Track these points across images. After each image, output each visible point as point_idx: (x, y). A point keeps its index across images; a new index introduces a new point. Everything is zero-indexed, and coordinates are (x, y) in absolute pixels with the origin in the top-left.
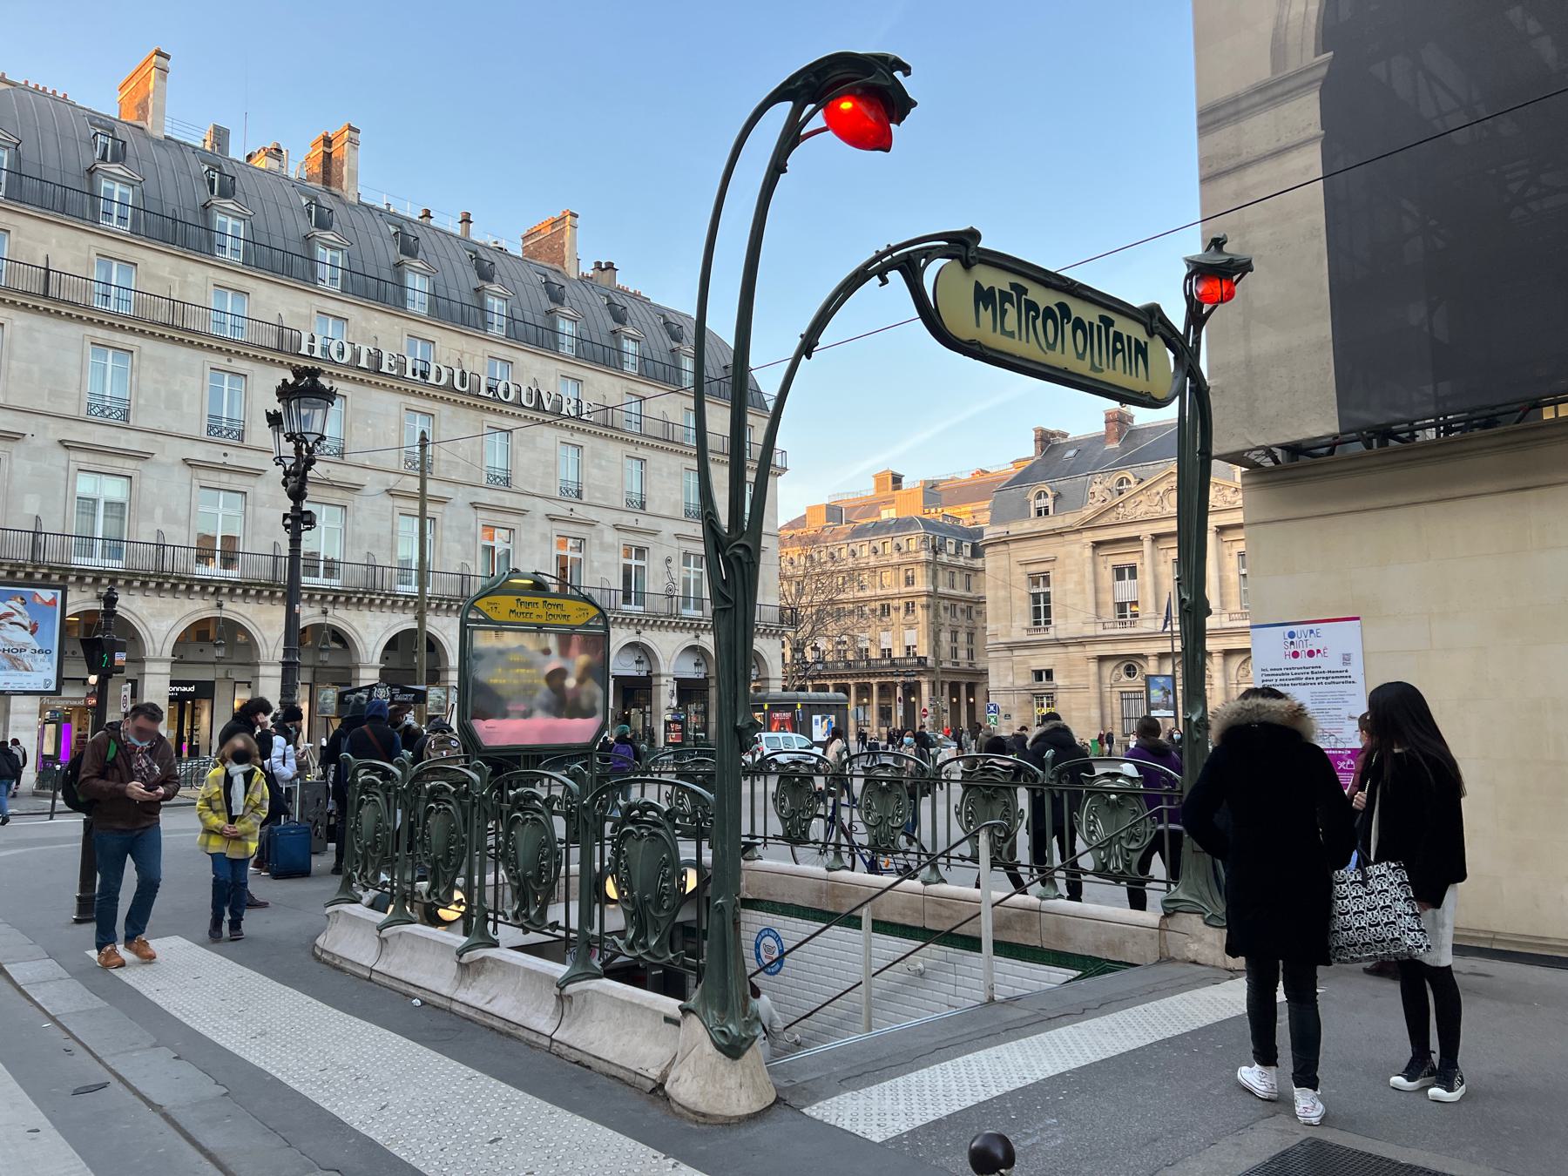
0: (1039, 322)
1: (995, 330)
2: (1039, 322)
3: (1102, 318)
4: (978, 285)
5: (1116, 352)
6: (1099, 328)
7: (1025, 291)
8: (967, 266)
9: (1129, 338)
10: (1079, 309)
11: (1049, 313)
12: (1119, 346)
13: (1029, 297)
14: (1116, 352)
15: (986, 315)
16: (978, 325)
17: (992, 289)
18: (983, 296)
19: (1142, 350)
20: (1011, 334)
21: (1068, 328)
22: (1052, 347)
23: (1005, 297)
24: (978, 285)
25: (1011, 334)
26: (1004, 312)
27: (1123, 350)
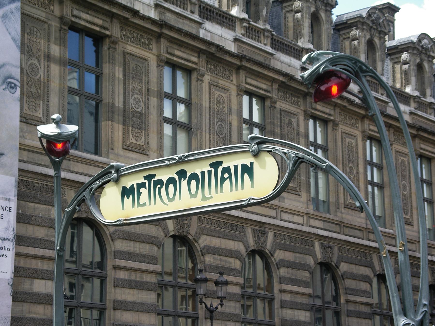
0: (163, 190)
2: (163, 190)
3: (211, 165)
4: (124, 188)
5: (223, 180)
6: (210, 172)
8: (117, 181)
9: (236, 167)
10: (190, 169)
11: (171, 180)
13: (157, 178)
15: (128, 201)
16: (123, 208)
17: (133, 186)
20: (145, 204)
21: (184, 183)
22: (173, 199)
24: (124, 188)
25: (145, 204)
26: (139, 194)
27: (230, 177)
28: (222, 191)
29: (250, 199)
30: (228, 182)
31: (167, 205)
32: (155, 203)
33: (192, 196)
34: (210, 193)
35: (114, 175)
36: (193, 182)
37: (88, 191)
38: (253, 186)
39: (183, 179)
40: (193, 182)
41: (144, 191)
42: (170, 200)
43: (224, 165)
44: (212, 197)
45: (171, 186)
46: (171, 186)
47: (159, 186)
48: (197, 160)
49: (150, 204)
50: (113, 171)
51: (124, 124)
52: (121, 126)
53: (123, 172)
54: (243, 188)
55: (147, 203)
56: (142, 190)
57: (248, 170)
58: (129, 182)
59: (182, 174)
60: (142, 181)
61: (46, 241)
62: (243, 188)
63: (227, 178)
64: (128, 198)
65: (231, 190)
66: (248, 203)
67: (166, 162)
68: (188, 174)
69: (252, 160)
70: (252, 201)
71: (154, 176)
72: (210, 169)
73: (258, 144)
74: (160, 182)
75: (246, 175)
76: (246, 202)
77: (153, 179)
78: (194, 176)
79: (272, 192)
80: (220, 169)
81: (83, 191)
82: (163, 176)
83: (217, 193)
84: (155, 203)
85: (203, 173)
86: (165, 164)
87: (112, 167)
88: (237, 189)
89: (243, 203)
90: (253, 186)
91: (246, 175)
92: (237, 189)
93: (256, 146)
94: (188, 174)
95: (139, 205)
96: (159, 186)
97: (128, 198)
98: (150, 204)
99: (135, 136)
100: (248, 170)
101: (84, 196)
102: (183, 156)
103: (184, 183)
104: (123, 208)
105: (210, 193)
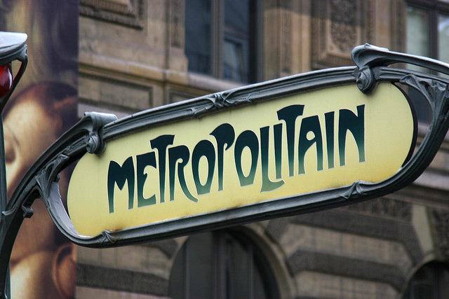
0: (188, 169)
1: (131, 206)
2: (188, 169)
3: (281, 114)
5: (305, 145)
6: (278, 128)
7: (170, 139)
8: (99, 151)
9: (329, 117)
11: (203, 148)
13: (176, 143)
15: (121, 194)
16: (111, 210)
17: (130, 159)
20: (152, 200)
21: (229, 154)
25: (152, 200)
26: (142, 178)
27: (318, 139)
28: (302, 170)
29: (355, 186)
30: (312, 150)
31: (195, 200)
32: (172, 198)
33: (245, 181)
34: (279, 175)
35: (94, 139)
36: (246, 152)
37: (43, 173)
38: (362, 159)
39: (226, 145)
40: (246, 152)
41: (152, 172)
43: (307, 113)
44: (282, 183)
45: (204, 161)
46: (204, 161)
47: (180, 161)
48: (254, 103)
49: (162, 200)
50: (90, 129)
51: (313, 13)
52: (306, 19)
53: (109, 131)
54: (342, 163)
55: (158, 198)
56: (148, 170)
57: (353, 122)
58: (120, 152)
59: (224, 134)
60: (150, 150)
61: (144, 275)
62: (342, 163)
63: (311, 142)
64: (121, 187)
65: (320, 167)
66: (352, 195)
67: (194, 110)
70: (360, 190)
71: (170, 139)
72: (278, 122)
73: (372, 65)
74: (182, 151)
75: (348, 132)
76: (348, 192)
77: (170, 146)
78: (248, 138)
79: (400, 169)
81: (35, 174)
82: (188, 135)
83: (291, 174)
84: (172, 198)
85: (265, 131)
86: (190, 113)
87: (89, 120)
88: (331, 165)
89: (343, 194)
90: (362, 159)
91: (349, 135)
92: (331, 165)
93: (368, 71)
95: (142, 202)
96: (180, 161)
97: (121, 187)
98: (162, 200)
99: (340, 41)
100: (353, 122)
101: (37, 184)
102: (225, 95)
103: (229, 154)
104: (111, 210)
105: (279, 175)
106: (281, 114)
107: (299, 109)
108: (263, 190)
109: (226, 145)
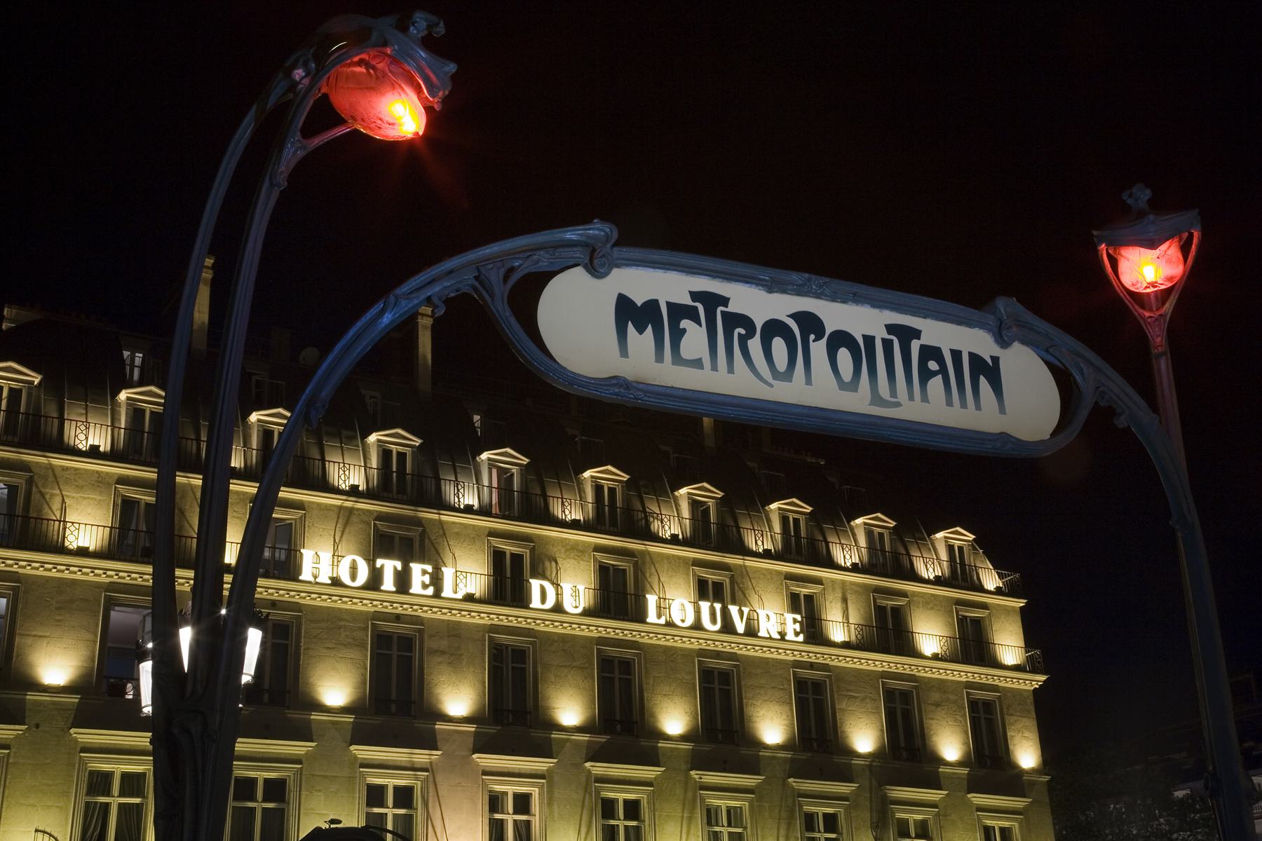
2: (755, 344)
5: (926, 375)
6: (887, 345)
9: (956, 355)
11: (774, 328)
12: (933, 366)
13: (732, 308)
14: (926, 375)
15: (642, 341)
16: (624, 351)
17: (652, 305)
18: (630, 314)
19: (987, 370)
20: (697, 363)
21: (819, 349)
22: (788, 375)
23: (678, 312)
25: (697, 363)
26: (678, 334)
27: (943, 370)
28: (925, 398)
30: (938, 379)
31: (771, 386)
34: (893, 392)
38: (1002, 409)
39: (812, 337)
40: (844, 355)
42: (776, 374)
43: (926, 339)
44: (898, 405)
45: (779, 344)
46: (779, 344)
47: (743, 331)
49: (714, 367)
54: (978, 407)
56: (685, 323)
57: (987, 370)
59: (810, 324)
62: (978, 407)
63: (935, 374)
64: (641, 330)
65: (949, 403)
68: (828, 332)
69: (996, 350)
71: (725, 301)
74: (745, 322)
75: (982, 380)
78: (840, 339)
80: (915, 346)
83: (911, 398)
84: (731, 369)
85: (869, 340)
88: (964, 404)
90: (1002, 409)
91: (982, 380)
92: (964, 404)
94: (828, 332)
95: (677, 359)
96: (743, 331)
97: (641, 330)
98: (714, 367)
104: (624, 351)
105: (893, 392)
106: (891, 328)
107: (917, 334)
108: (871, 404)
109: (812, 337)
